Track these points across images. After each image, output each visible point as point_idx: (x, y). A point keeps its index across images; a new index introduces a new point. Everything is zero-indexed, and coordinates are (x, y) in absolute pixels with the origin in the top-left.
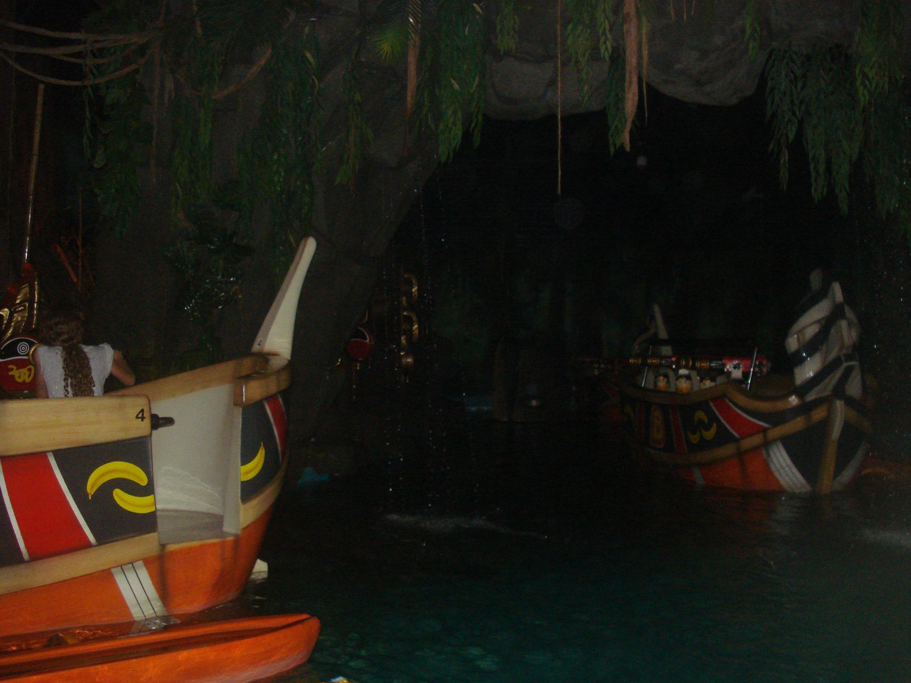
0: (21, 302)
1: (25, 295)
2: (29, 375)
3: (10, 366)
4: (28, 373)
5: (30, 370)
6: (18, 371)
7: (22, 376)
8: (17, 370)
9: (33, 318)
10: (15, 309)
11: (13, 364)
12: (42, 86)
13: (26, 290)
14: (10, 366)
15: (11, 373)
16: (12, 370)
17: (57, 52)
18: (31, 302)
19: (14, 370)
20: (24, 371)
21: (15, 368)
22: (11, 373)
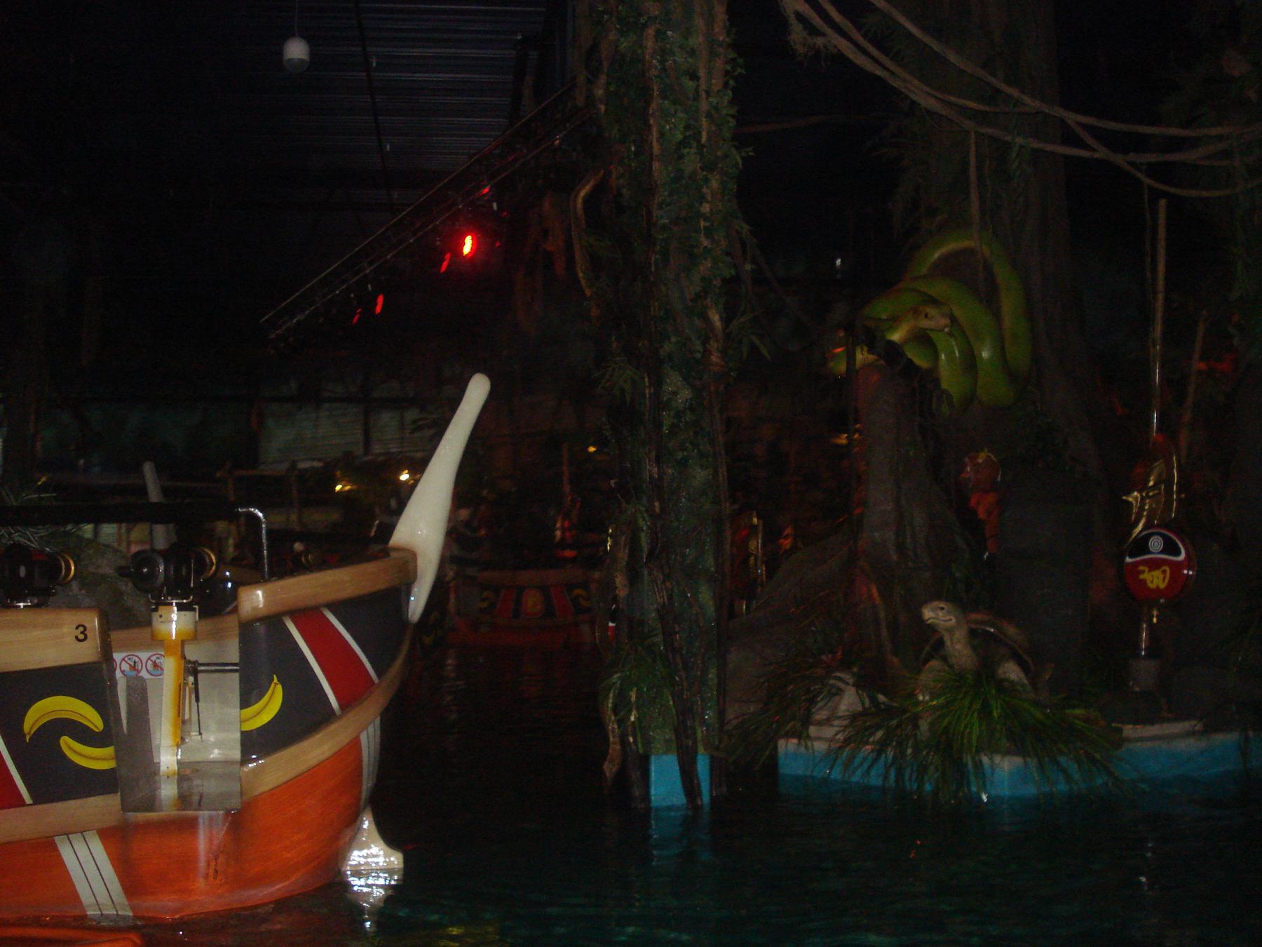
0: (1155, 484)
1: (1160, 475)
2: (1164, 578)
3: (1141, 568)
4: (1161, 576)
5: (1164, 572)
6: (1150, 574)
7: (1155, 581)
8: (1150, 571)
9: (1173, 504)
10: (1147, 494)
11: (1144, 565)
12: (1163, 202)
13: (1159, 466)
14: (1141, 568)
15: (1142, 577)
16: (1143, 572)
17: (1190, 156)
18: (1169, 483)
19: (1146, 572)
20: (1157, 573)
21: (1147, 569)
22: (1142, 577)
